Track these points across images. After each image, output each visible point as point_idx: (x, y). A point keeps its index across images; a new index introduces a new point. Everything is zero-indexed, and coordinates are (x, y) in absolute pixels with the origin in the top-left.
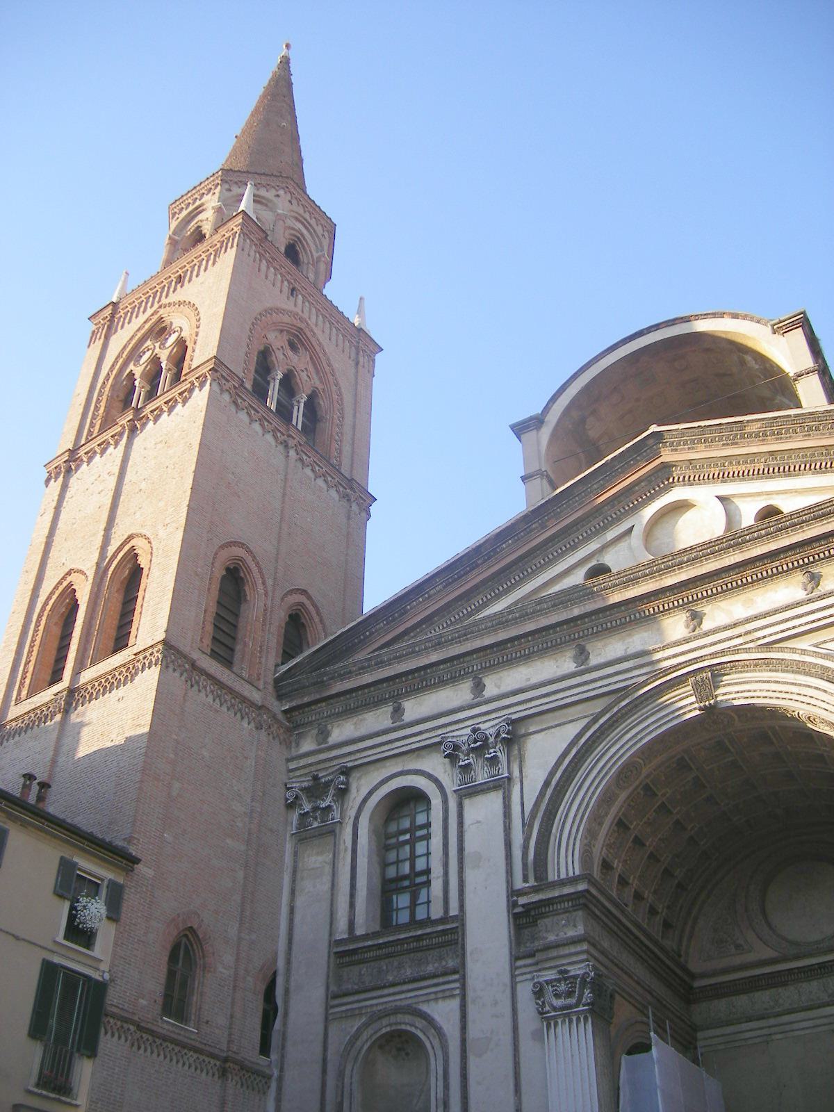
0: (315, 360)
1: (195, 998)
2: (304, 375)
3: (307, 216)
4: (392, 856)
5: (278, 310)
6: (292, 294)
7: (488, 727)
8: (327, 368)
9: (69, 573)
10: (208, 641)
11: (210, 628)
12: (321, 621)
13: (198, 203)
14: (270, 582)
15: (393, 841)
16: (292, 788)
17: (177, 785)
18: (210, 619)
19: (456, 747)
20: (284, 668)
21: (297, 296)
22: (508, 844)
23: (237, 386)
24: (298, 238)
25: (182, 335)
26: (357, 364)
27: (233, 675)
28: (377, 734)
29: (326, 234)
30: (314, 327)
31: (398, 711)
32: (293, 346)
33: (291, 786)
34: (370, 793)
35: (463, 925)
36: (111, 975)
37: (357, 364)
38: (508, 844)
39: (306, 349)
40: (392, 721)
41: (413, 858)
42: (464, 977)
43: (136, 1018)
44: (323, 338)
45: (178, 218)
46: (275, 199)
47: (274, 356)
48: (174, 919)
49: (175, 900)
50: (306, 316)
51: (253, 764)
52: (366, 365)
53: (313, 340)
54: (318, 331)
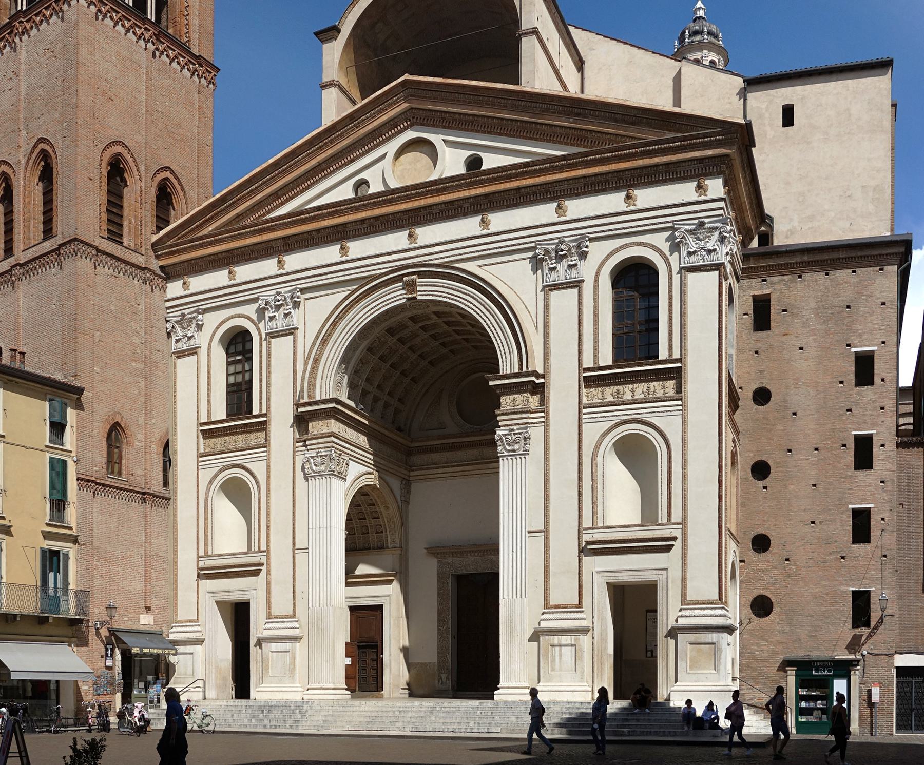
10: (105, 227)
11: (105, 217)
17: (98, 334)
19: (267, 303)
22: (295, 372)
27: (124, 249)
36: (77, 458)
38: (295, 372)
42: (268, 452)
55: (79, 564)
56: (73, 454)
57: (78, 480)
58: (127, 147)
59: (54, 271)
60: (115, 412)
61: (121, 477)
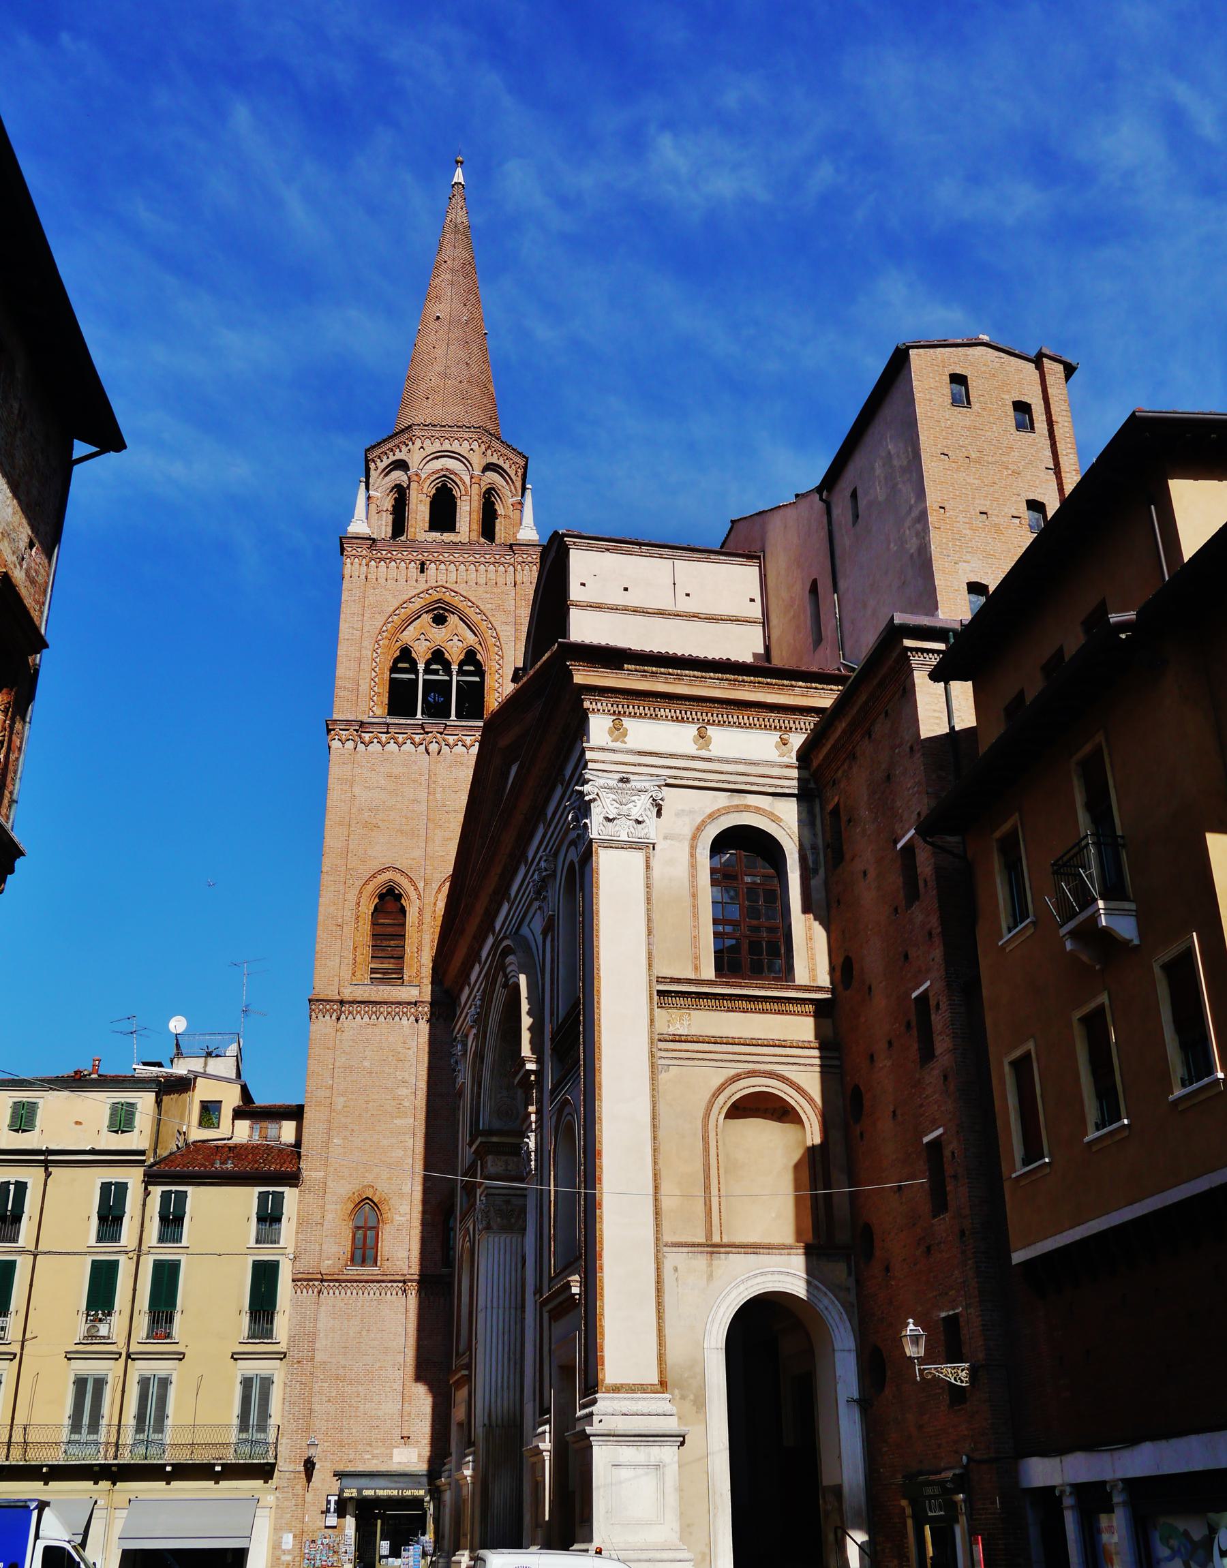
3: (446, 446)
6: (422, 571)
8: (477, 618)
14: (421, 885)
23: (357, 728)
32: (440, 620)
39: (453, 613)
47: (413, 652)
48: (349, 1198)
53: (456, 600)
55: (289, 1389)
57: (293, 1281)
60: (365, 1186)
61: (377, 1266)
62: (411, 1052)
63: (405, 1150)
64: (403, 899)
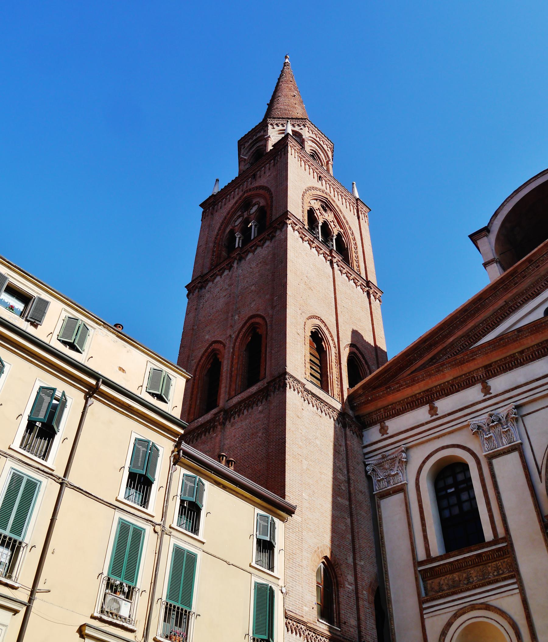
0: (336, 216)
1: (335, 606)
2: (332, 224)
3: (318, 139)
4: (445, 503)
5: (313, 188)
7: (502, 412)
8: (344, 220)
9: (211, 345)
11: (308, 365)
12: (367, 363)
13: (255, 138)
15: (443, 493)
16: (369, 464)
18: (308, 360)
20: (352, 390)
21: (322, 180)
23: (302, 227)
24: (315, 152)
25: (261, 205)
26: (359, 218)
28: (422, 425)
29: (329, 149)
30: (333, 198)
31: (433, 410)
33: (368, 463)
34: (424, 462)
35: (511, 545)
37: (359, 218)
39: (331, 210)
40: (430, 416)
41: (460, 503)
43: (304, 620)
44: (339, 203)
45: (244, 147)
46: (300, 131)
48: (315, 551)
49: (315, 538)
50: (328, 191)
51: (345, 449)
52: (363, 218)
54: (336, 199)
56: (281, 583)
58: (324, 322)
59: (260, 408)
62: (342, 449)
63: (346, 525)
64: (323, 342)
